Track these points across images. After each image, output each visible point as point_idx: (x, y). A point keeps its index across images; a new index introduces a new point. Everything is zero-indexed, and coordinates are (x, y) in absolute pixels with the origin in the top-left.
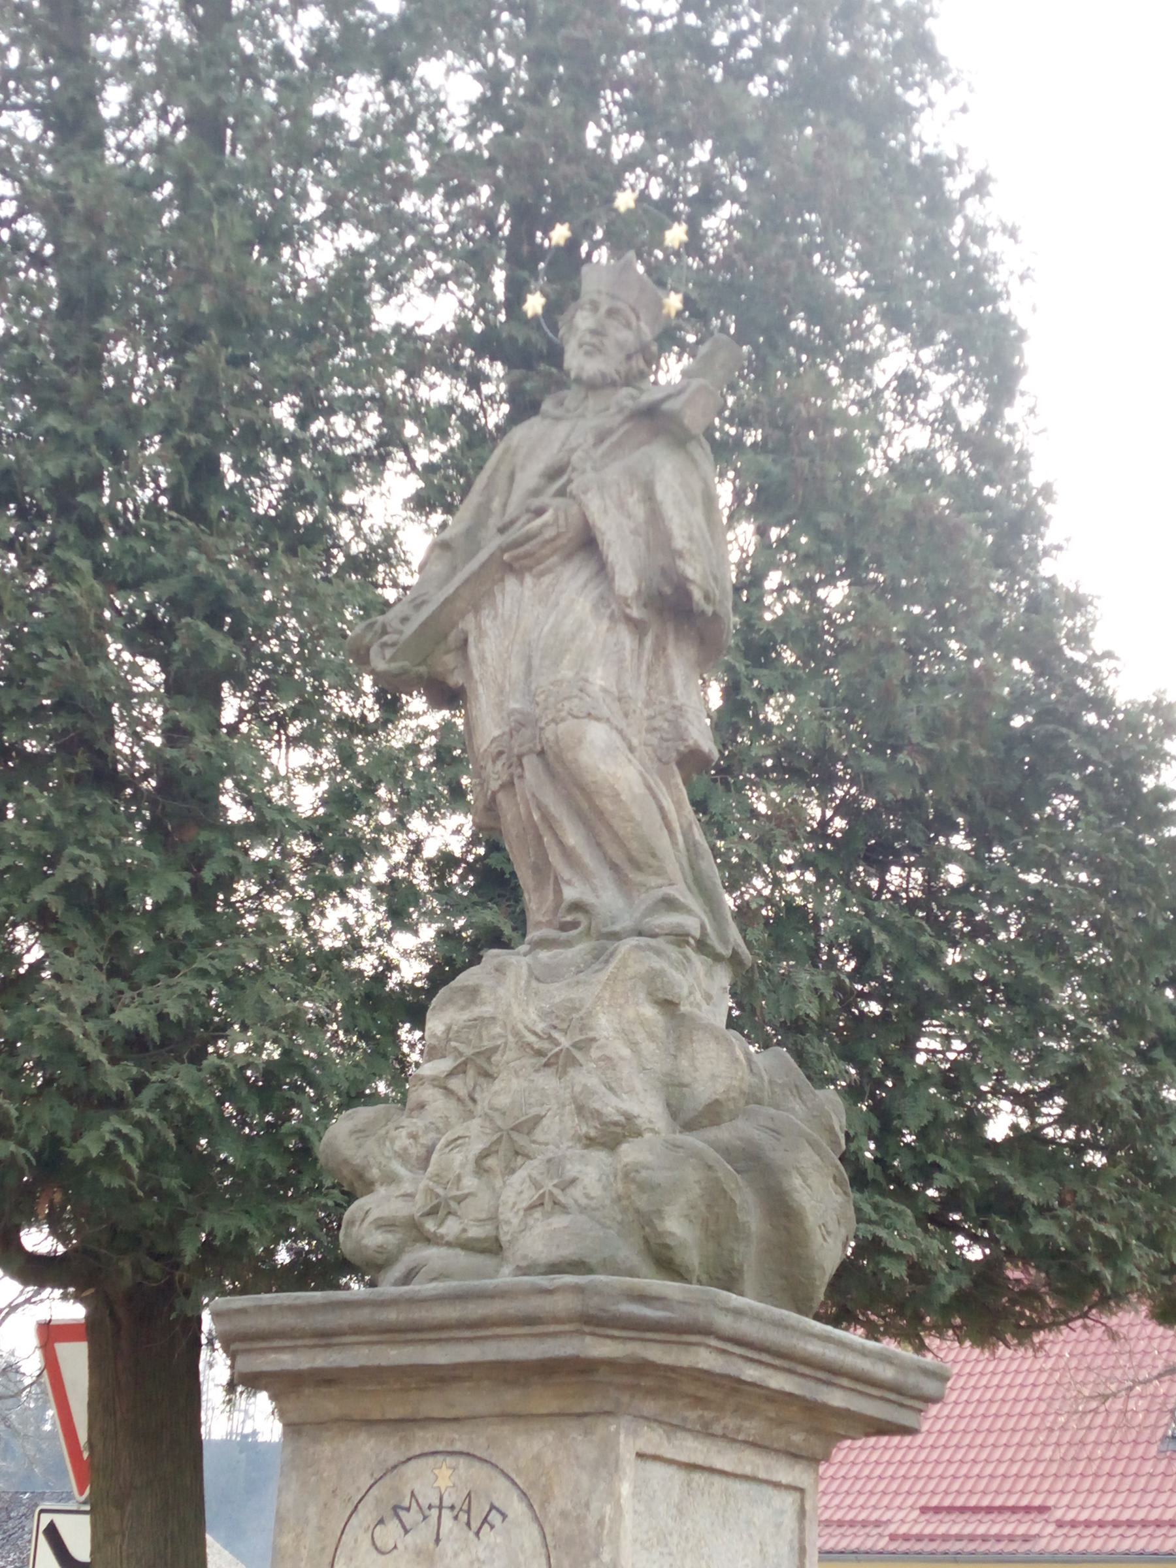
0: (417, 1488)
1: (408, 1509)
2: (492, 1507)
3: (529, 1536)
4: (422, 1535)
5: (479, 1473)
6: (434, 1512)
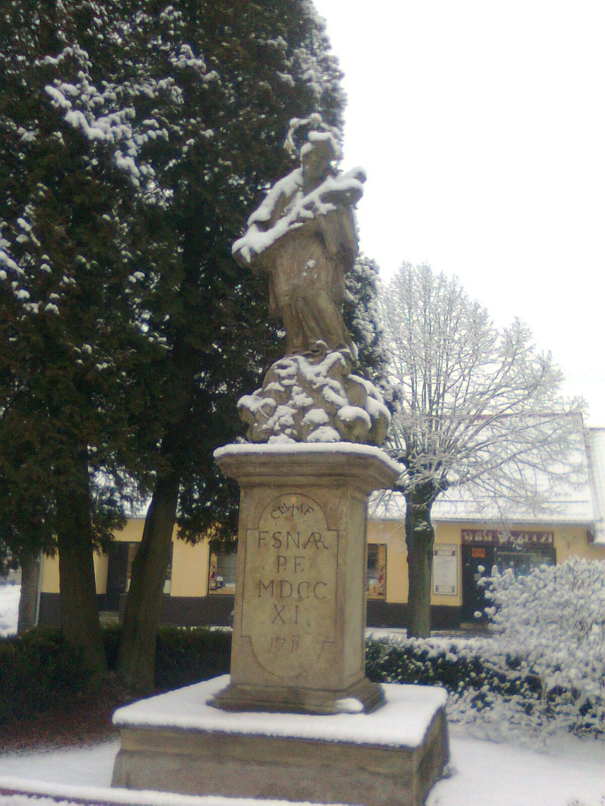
0: (285, 502)
1: (283, 507)
2: (309, 507)
3: (320, 515)
4: (288, 514)
5: (304, 499)
6: (292, 508)
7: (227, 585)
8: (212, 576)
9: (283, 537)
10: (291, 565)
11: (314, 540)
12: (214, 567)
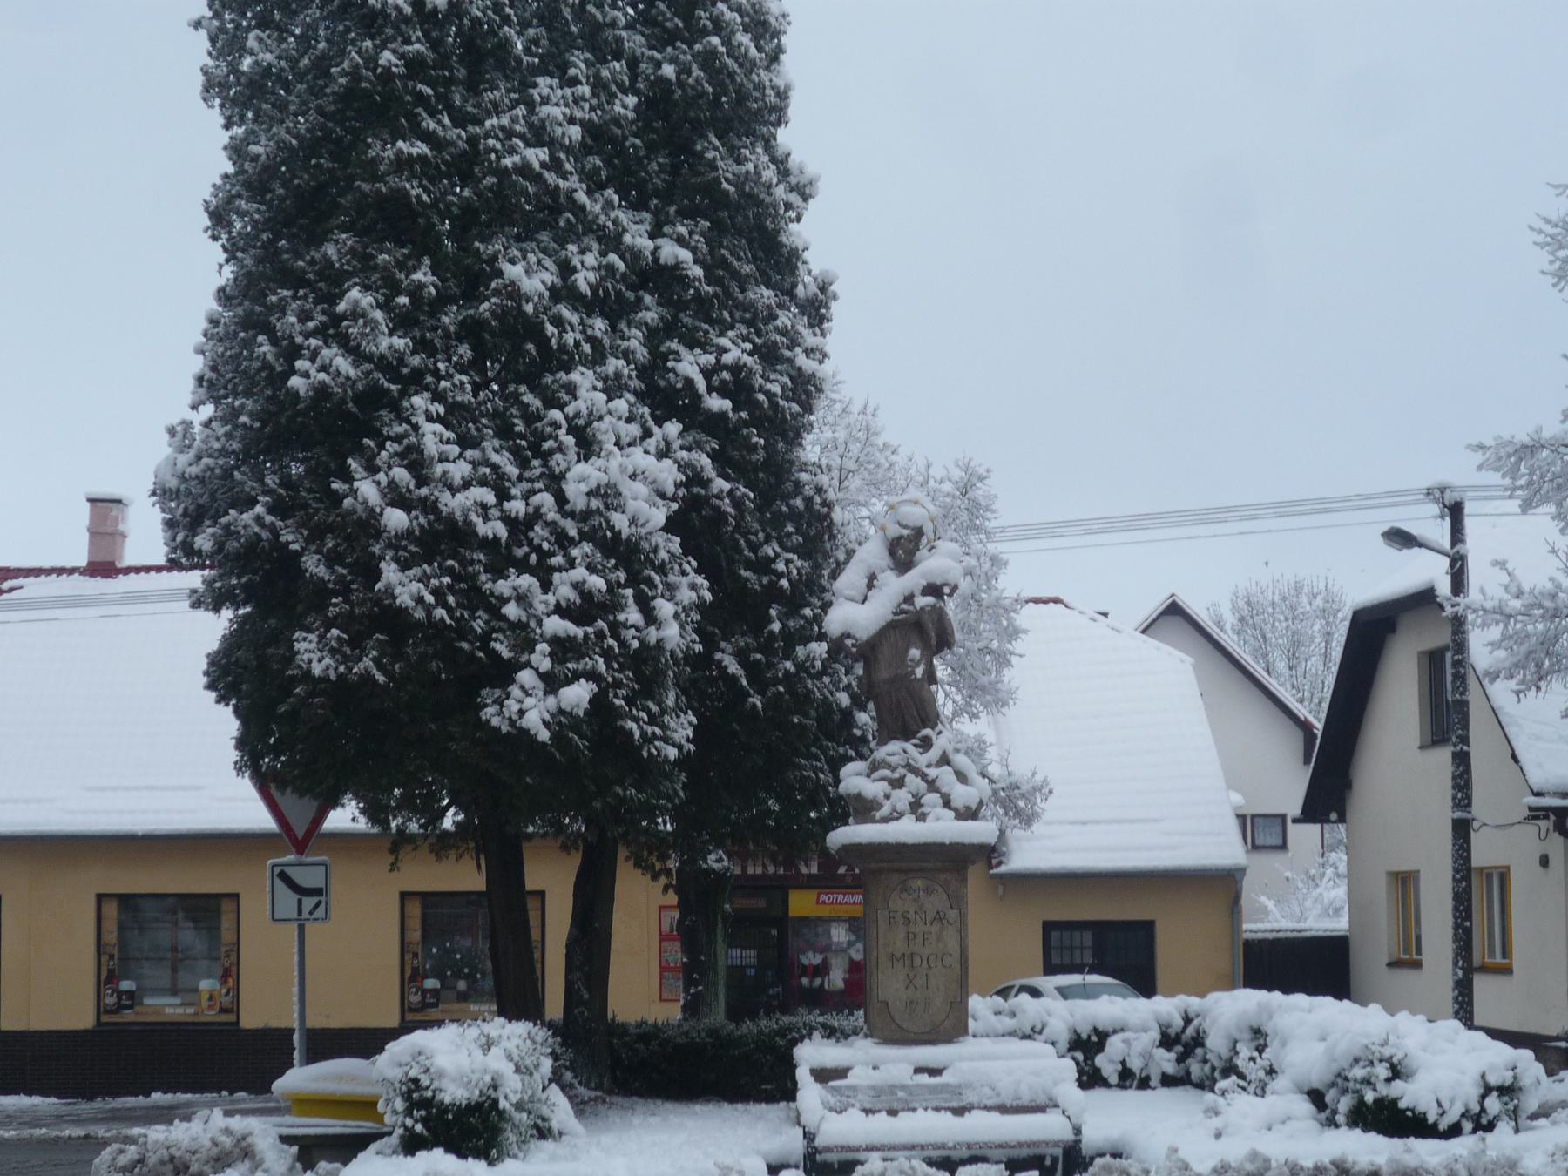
7: (148, 1001)
8: (106, 979)
9: (911, 916)
10: (920, 939)
11: (939, 917)
12: (415, 955)
